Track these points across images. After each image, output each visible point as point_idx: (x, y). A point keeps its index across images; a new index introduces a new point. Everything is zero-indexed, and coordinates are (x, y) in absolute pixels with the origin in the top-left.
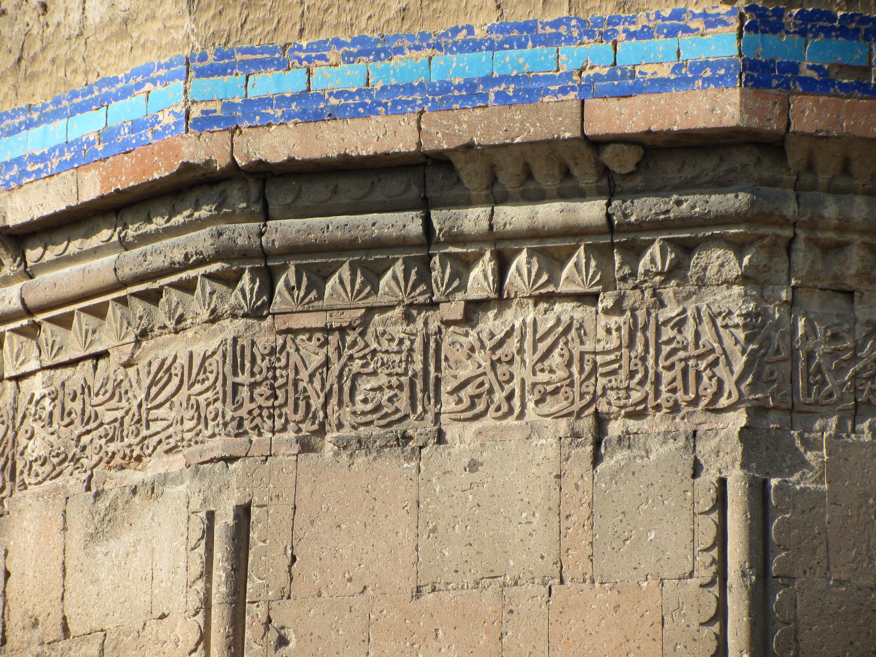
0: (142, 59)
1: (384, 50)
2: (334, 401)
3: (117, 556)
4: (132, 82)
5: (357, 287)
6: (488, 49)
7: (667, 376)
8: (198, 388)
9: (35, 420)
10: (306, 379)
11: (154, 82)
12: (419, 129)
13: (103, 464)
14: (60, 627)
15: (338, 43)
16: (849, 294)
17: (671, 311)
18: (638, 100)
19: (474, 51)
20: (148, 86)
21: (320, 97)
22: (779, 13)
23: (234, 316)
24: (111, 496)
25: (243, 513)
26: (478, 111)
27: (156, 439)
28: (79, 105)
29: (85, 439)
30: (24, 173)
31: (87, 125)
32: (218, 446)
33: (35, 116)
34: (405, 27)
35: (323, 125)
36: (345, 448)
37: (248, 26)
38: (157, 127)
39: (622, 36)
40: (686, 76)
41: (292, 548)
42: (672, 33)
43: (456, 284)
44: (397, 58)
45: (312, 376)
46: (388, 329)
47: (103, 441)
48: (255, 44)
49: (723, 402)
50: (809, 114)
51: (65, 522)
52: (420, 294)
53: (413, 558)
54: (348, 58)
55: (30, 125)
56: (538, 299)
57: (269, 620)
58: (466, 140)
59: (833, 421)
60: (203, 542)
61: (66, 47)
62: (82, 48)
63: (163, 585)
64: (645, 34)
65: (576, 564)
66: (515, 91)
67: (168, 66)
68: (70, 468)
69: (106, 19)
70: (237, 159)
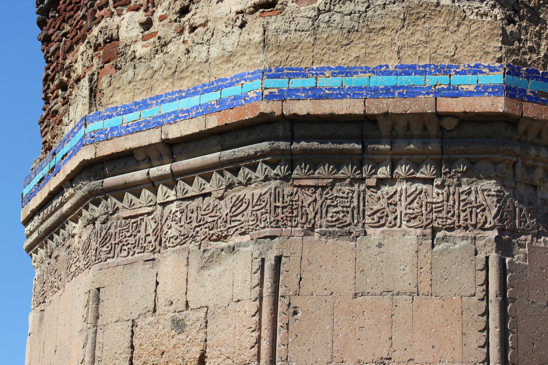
0: (240, 71)
1: (350, 72)
2: (318, 216)
3: (215, 276)
4: (234, 80)
5: (330, 169)
6: (395, 75)
7: (462, 215)
8: (257, 208)
9: (172, 221)
10: (307, 206)
11: (245, 80)
12: (365, 105)
13: (207, 239)
14: (184, 306)
15: (329, 68)
16: (535, 187)
17: (465, 188)
18: (460, 99)
19: (389, 75)
20: (242, 82)
21: (321, 89)
22: (519, 69)
23: (275, 179)
24: (211, 252)
25: (278, 259)
26: (390, 100)
27: (235, 228)
28: (207, 89)
29: (197, 229)
30: (177, 117)
31: (212, 97)
32: (268, 231)
33: (184, 94)
34: (358, 64)
35: (323, 101)
36: (324, 235)
37: (289, 59)
38: (247, 98)
39: (453, 73)
40: (481, 91)
41: (300, 275)
42: (475, 73)
43: (373, 171)
44: (355, 76)
45: (309, 205)
46: (342, 188)
47: (207, 229)
48: (293, 66)
49: (487, 226)
50: (531, 110)
51: (188, 262)
52: (358, 174)
53: (353, 282)
54: (334, 75)
55: (181, 98)
56: (407, 180)
57: (290, 304)
58: (386, 110)
59: (530, 237)
60: (259, 271)
61: (199, 67)
62: (207, 67)
63: (239, 288)
64: (463, 73)
65: (424, 288)
66: (407, 92)
67: (253, 74)
68: (190, 241)
69: (220, 55)
70: (284, 112)
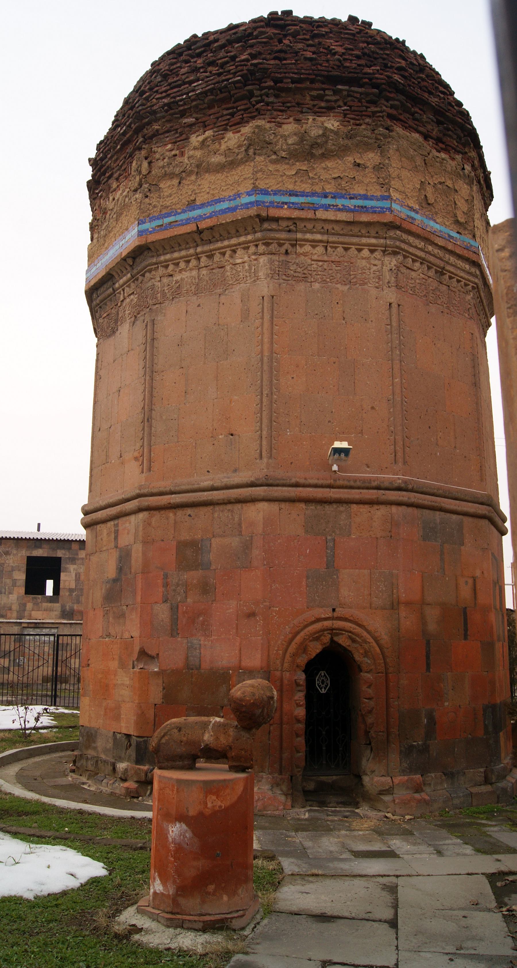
16: (171, 275)
22: (145, 220)
